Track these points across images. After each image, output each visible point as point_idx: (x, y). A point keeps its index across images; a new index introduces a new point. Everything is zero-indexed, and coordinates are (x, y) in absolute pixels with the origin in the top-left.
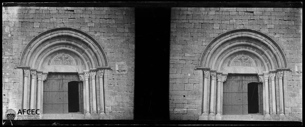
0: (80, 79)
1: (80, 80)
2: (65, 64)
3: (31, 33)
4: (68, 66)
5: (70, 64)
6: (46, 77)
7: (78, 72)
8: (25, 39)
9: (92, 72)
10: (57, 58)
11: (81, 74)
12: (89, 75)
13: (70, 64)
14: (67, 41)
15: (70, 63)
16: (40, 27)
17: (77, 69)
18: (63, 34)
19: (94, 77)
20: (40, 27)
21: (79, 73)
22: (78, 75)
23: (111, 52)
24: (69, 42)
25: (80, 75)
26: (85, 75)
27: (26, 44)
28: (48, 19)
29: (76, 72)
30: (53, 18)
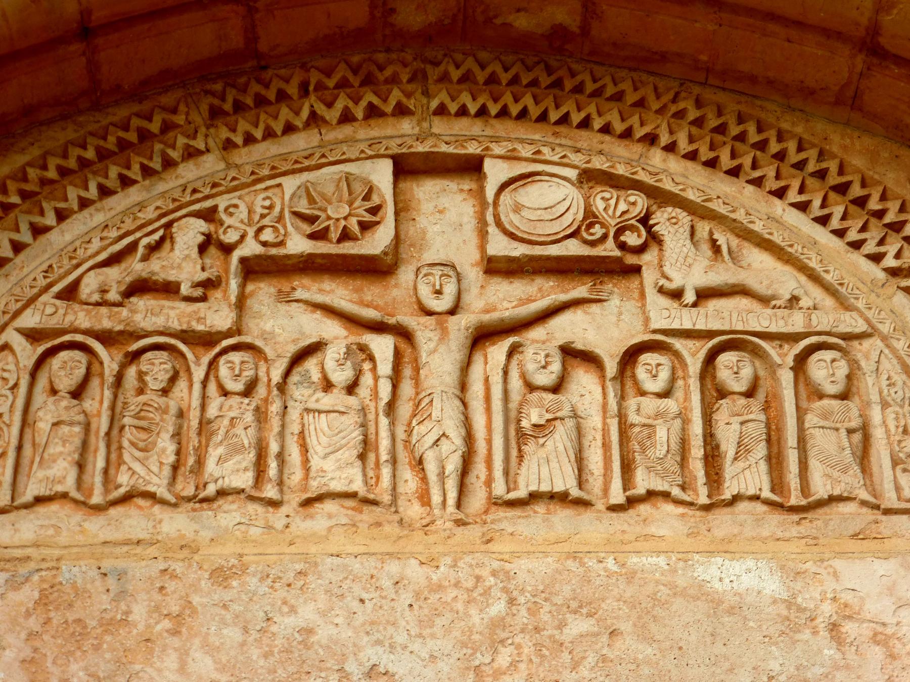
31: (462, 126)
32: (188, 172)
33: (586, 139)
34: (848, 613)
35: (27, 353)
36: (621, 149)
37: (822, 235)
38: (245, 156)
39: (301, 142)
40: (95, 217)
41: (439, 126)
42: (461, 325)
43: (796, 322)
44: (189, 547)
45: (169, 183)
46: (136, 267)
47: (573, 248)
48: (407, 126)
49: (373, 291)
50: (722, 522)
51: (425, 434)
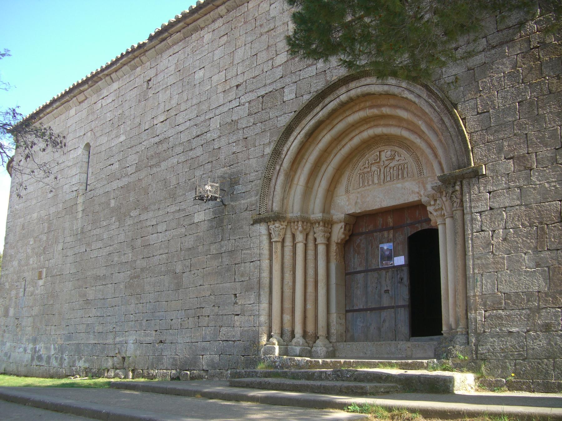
4: (395, 182)
5: (400, 177)
6: (343, 229)
13: (400, 177)
14: (372, 110)
15: (400, 172)
17: (419, 187)
18: (352, 95)
21: (422, 200)
24: (375, 111)
31: (384, 147)
32: (367, 156)
33: (391, 146)
34: (405, 187)
35: (359, 176)
36: (393, 147)
37: (406, 153)
38: (370, 154)
39: (373, 151)
40: (361, 162)
41: (382, 148)
42: (384, 166)
43: (404, 162)
44: (368, 189)
45: (366, 158)
46: (364, 166)
47: (390, 158)
48: (380, 148)
49: (379, 164)
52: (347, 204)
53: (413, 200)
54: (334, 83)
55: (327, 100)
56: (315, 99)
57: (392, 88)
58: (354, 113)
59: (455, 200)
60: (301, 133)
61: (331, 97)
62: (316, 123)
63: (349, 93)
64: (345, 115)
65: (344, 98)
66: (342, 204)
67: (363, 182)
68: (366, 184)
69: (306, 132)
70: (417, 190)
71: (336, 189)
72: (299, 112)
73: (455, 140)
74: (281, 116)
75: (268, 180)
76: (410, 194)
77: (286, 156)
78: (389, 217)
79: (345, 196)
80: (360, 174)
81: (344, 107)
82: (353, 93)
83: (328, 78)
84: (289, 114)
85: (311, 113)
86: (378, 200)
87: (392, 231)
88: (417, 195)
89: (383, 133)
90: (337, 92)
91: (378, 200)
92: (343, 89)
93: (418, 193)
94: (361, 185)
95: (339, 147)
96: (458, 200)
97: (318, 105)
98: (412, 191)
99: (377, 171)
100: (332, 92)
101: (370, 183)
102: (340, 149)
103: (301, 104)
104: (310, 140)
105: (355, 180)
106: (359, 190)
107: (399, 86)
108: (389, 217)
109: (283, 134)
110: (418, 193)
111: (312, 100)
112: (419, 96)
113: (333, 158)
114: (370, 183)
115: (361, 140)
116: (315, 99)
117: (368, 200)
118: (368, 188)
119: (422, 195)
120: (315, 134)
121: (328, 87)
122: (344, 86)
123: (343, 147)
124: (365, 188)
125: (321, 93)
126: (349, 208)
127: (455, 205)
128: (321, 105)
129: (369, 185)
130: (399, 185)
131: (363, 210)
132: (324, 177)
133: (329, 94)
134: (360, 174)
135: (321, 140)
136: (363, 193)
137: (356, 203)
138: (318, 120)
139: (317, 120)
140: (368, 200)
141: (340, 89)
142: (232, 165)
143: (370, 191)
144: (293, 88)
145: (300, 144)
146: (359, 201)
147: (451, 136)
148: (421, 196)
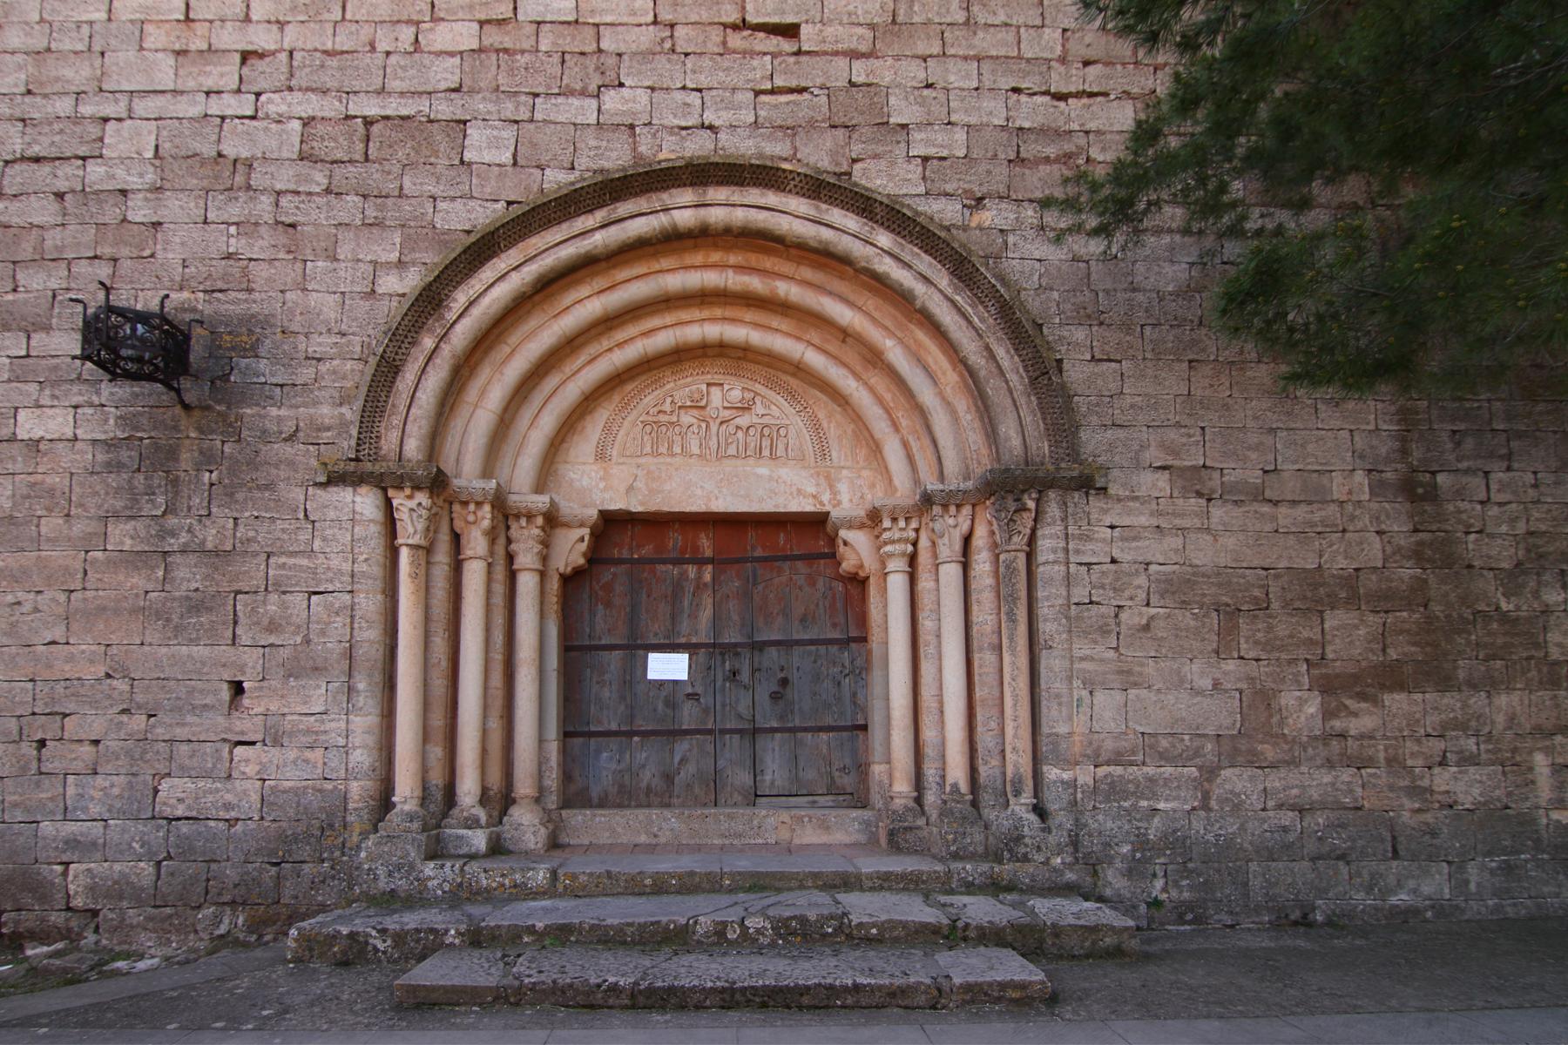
0: (843, 559)
1: (844, 565)
2: (732, 450)
3: (442, 205)
4: (751, 461)
7: (827, 508)
8: (394, 256)
9: (937, 510)
10: (667, 407)
11: (850, 527)
12: (912, 535)
16: (515, 164)
17: (818, 485)
18: (712, 220)
19: (958, 546)
20: (521, 161)
21: (835, 514)
22: (829, 528)
23: (1098, 356)
25: (843, 533)
26: (886, 535)
27: (404, 295)
28: (583, 93)
29: (809, 508)
30: (621, 85)
35: (641, 426)
44: (671, 464)
50: (761, 461)
51: (711, 443)
52: (602, 485)
53: (800, 510)
54: (668, 169)
55: (624, 208)
56: (591, 190)
57: (846, 239)
58: (686, 268)
59: (1021, 528)
60: (526, 269)
61: (641, 204)
62: (579, 256)
63: (702, 212)
64: (657, 267)
65: (685, 218)
66: (584, 483)
67: (655, 444)
68: (663, 450)
69: (541, 270)
70: (811, 489)
71: (565, 445)
72: (533, 209)
73: (1022, 401)
74: (453, 199)
75: (387, 370)
76: (791, 494)
77: (460, 316)
78: (703, 535)
79: (594, 467)
80: (645, 424)
81: (673, 241)
82: (716, 216)
83: (643, 149)
84: (488, 204)
85: (565, 226)
86: (699, 492)
87: (710, 568)
88: (811, 500)
89: (704, 338)
90: (665, 196)
91: (699, 492)
92: (687, 196)
93: (814, 497)
94: (648, 449)
95: (606, 343)
96: (1028, 531)
97: (591, 211)
98: (799, 491)
99: (700, 426)
100: (647, 191)
101: (677, 450)
102: (610, 350)
103: (535, 188)
104: (537, 298)
105: (627, 434)
106: (642, 460)
107: (867, 242)
108: (703, 535)
109: (464, 252)
110: (814, 497)
111: (582, 188)
112: (926, 280)
113: (584, 366)
114: (677, 450)
115: (704, 338)
116: (591, 190)
117: (667, 487)
118: (669, 460)
119: (826, 502)
120: (555, 287)
121: (647, 173)
122: (690, 190)
123: (620, 345)
124: (661, 459)
125: (619, 179)
126: (607, 496)
127: (1016, 539)
128: (600, 215)
129: (673, 455)
130: (763, 471)
131: (652, 508)
132: (550, 406)
133: (636, 195)
134: (645, 424)
135: (568, 308)
136: (653, 468)
137: (630, 489)
138: (587, 252)
139: (582, 251)
140: (667, 487)
141: (674, 191)
142: (220, 291)
143: (676, 469)
144: (504, 134)
145: (514, 300)
146: (639, 484)
147: (1010, 391)
148: (821, 503)
